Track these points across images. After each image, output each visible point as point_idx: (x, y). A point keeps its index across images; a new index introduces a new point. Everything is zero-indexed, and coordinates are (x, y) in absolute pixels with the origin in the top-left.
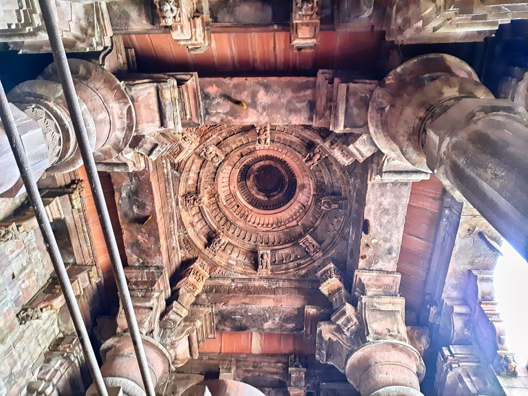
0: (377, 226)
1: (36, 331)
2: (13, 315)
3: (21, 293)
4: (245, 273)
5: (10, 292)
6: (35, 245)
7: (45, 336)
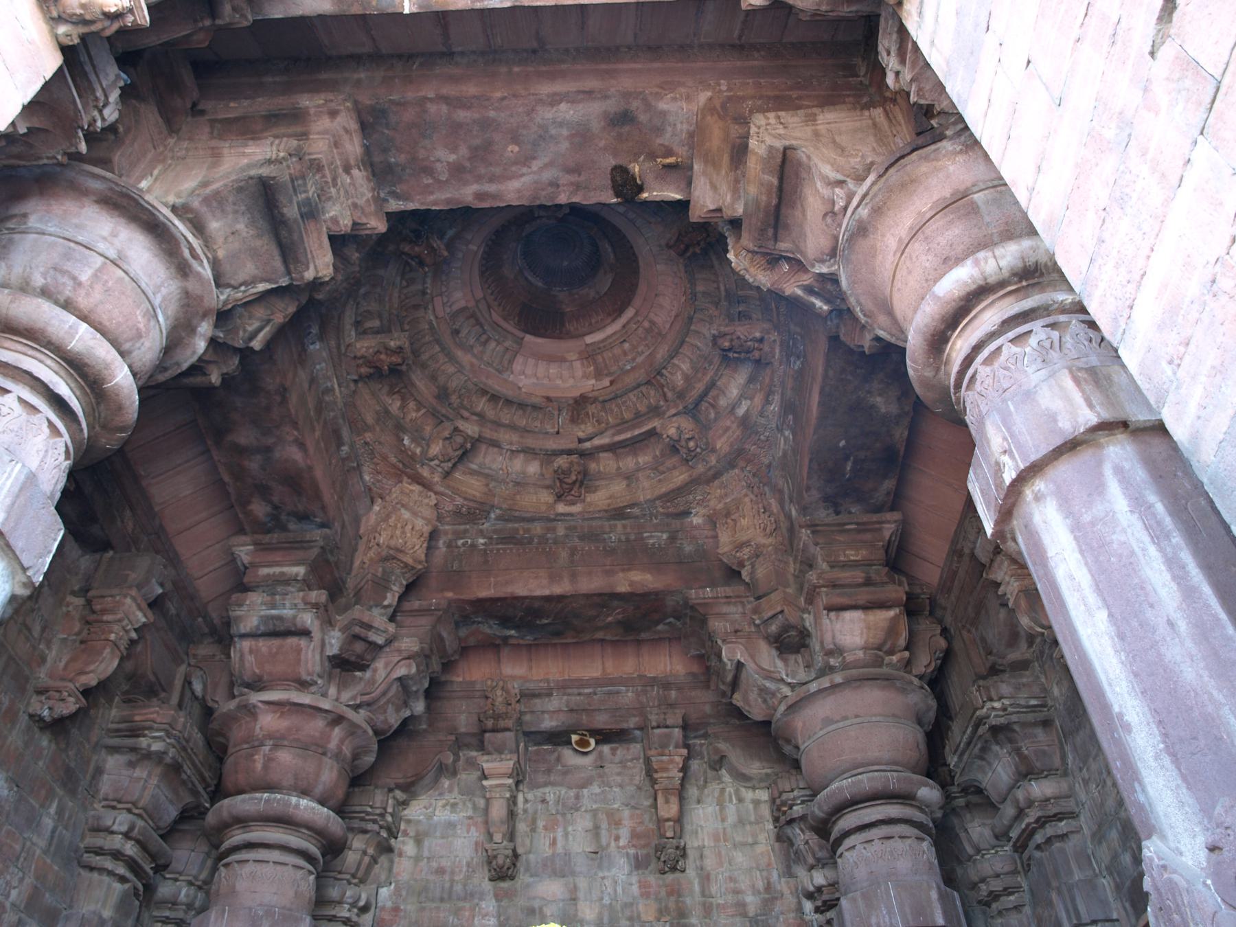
0: (535, 168)
1: (722, 843)
2: (653, 879)
3: (632, 851)
4: (769, 393)
5: (614, 871)
6: (572, 793)
7: (748, 827)
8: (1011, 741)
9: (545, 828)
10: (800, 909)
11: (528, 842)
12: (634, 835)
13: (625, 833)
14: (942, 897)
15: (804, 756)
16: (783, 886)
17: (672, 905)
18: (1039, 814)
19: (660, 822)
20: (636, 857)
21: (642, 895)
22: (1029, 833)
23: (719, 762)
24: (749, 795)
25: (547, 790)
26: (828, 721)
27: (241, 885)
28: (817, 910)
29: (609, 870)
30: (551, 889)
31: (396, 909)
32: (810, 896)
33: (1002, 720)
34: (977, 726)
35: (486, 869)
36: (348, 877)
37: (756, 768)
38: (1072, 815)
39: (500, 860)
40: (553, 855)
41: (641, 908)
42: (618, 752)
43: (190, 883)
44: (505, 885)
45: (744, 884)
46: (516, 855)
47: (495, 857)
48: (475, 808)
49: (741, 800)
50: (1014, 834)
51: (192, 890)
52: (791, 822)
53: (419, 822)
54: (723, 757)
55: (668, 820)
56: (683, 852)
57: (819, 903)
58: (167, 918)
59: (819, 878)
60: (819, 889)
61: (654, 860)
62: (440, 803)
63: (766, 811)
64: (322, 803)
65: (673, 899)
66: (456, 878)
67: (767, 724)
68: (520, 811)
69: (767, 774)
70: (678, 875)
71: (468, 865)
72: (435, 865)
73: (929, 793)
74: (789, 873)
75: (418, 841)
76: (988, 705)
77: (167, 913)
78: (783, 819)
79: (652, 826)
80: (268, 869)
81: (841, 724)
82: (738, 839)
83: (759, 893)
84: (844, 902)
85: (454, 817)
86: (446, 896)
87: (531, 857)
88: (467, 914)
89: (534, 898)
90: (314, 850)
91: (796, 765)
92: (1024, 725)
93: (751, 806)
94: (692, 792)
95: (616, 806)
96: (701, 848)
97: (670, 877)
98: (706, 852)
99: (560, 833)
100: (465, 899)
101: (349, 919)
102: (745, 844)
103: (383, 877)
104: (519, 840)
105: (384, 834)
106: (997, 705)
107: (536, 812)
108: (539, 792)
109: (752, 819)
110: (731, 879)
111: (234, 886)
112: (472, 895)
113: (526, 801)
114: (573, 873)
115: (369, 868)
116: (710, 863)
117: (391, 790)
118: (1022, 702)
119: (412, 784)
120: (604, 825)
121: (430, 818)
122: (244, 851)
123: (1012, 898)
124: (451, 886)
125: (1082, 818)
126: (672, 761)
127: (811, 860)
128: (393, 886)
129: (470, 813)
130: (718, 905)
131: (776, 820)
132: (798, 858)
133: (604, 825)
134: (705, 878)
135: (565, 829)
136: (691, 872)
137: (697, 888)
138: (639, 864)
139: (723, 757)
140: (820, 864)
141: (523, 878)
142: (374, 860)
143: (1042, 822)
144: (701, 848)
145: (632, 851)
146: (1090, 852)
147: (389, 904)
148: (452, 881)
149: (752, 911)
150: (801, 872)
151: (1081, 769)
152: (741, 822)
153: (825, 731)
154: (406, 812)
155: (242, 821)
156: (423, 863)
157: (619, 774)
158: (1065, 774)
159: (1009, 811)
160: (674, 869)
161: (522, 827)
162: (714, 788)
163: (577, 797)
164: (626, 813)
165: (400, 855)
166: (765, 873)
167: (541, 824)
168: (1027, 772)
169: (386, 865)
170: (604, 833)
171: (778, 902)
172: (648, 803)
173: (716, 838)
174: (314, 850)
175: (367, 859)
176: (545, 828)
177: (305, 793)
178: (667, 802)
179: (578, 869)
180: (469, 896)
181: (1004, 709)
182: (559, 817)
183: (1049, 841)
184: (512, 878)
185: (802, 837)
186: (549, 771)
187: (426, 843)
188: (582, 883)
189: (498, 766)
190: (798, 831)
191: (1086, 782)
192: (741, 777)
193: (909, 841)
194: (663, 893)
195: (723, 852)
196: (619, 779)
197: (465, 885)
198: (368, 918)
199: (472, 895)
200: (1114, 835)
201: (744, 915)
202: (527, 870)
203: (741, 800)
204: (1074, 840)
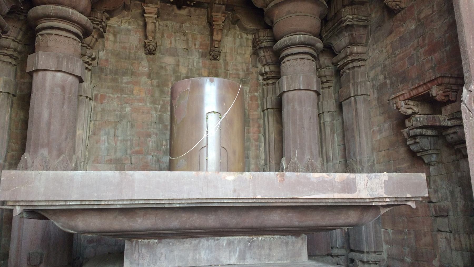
1: (233, 52)
2: (208, 62)
3: (200, 50)
5: (193, 57)
6: (178, 25)
7: (243, 48)
8: (351, 31)
9: (167, 37)
10: (258, 79)
11: (160, 41)
12: (201, 44)
13: (198, 43)
14: (317, 81)
15: (276, 25)
16: (254, 70)
17: (213, 71)
18: (353, 58)
19: (212, 41)
20: (202, 53)
21: (203, 67)
22: (347, 64)
23: (236, 21)
24: (245, 36)
25: (168, 22)
26: (289, 12)
27: (51, 44)
28: (264, 80)
29: (191, 56)
30: (169, 60)
31: (107, 60)
32: (262, 75)
33: (350, 23)
34: (339, 24)
35: (143, 49)
36: (86, 45)
37: (250, 26)
38: (364, 60)
39: (151, 47)
40: (170, 47)
41: (203, 71)
42: (197, 11)
43: (13, 40)
44: (151, 56)
45: (240, 67)
46: (157, 46)
47: (149, 45)
48: (138, 25)
49: (242, 37)
50: (340, 64)
51: (16, 44)
52: (260, 48)
53: (114, 27)
54: (238, 20)
55: (216, 41)
56: (219, 52)
57: (265, 77)
58: (6, 53)
59: (267, 69)
60: (266, 73)
61: (209, 55)
62: (124, 21)
63: (250, 43)
64: (82, 13)
65: (214, 69)
66: (131, 51)
67: (261, 10)
68: (157, 29)
69: (254, 29)
70: (217, 61)
71: (136, 47)
72: (122, 45)
73: (320, 45)
74: (255, 66)
75: (115, 35)
76: (348, 16)
77: (6, 52)
78: (258, 47)
79: (208, 42)
80: (62, 39)
81: (295, 14)
82: (239, 51)
83: (244, 71)
84: (284, 79)
85: (130, 27)
86: (127, 57)
87: (162, 47)
88: (136, 65)
89: (163, 63)
90: (81, 34)
91: (269, 27)
92: (358, 26)
93: (245, 40)
94: (225, 31)
95: (195, 32)
96: (226, 53)
97: (213, 61)
98: (228, 55)
99: (173, 40)
100: (135, 60)
101: (88, 62)
102: (241, 54)
103: (100, 47)
104: (157, 40)
105: (102, 30)
106: (351, 17)
107: (163, 30)
108: (165, 22)
109: (245, 45)
110: (235, 65)
111: (47, 44)
112: (138, 58)
113: (159, 25)
114: (178, 55)
115: (94, 44)
116: (228, 58)
117: (103, 12)
118: (360, 17)
119: (113, 10)
120: (190, 39)
121: (119, 26)
122: (49, 30)
123: (328, 84)
124: (130, 54)
125: (367, 61)
126: (220, 18)
127: (264, 63)
128: (105, 51)
129: (136, 26)
130: (230, 74)
131: (254, 47)
132: (261, 61)
133: (190, 39)
134: (226, 64)
135: (175, 38)
136: (221, 61)
137: (223, 66)
138: (203, 55)
139: (238, 20)
140: (267, 64)
141: (158, 55)
142: (97, 40)
143: (352, 61)
144: (226, 53)
145: (200, 50)
146: (366, 73)
147: (104, 58)
148: (130, 52)
149: (241, 77)
150: (260, 66)
151: (373, 45)
152: (241, 45)
153: (287, 16)
154: (108, 22)
155: (48, 17)
156: (117, 44)
157: (197, 20)
158: (366, 46)
159: (342, 55)
160: (215, 59)
161: (158, 35)
162: (232, 31)
163: (181, 26)
164: (199, 36)
165: (107, 40)
166: (247, 65)
167: (166, 35)
168: (352, 43)
169: (101, 43)
170: (190, 42)
171: (251, 75)
172: (208, 33)
173: (231, 50)
174: (81, 34)
175: (94, 40)
176: (167, 37)
177: (74, 8)
178: (217, 34)
179: (180, 54)
180: (136, 59)
181: (353, 19)
182: (173, 33)
183: (354, 67)
184: (154, 54)
185: (262, 53)
186: (169, 14)
187: (118, 36)
188: (181, 60)
189: (151, 10)
190: (262, 52)
191: (374, 49)
192: (244, 29)
193: (309, 61)
194: (211, 67)
195: (233, 56)
196: (196, 22)
197: (135, 55)
198: (95, 62)
199: (138, 58)
200: (379, 68)
201: (239, 78)
202: (160, 52)
203: (242, 37)
204: (362, 68)
